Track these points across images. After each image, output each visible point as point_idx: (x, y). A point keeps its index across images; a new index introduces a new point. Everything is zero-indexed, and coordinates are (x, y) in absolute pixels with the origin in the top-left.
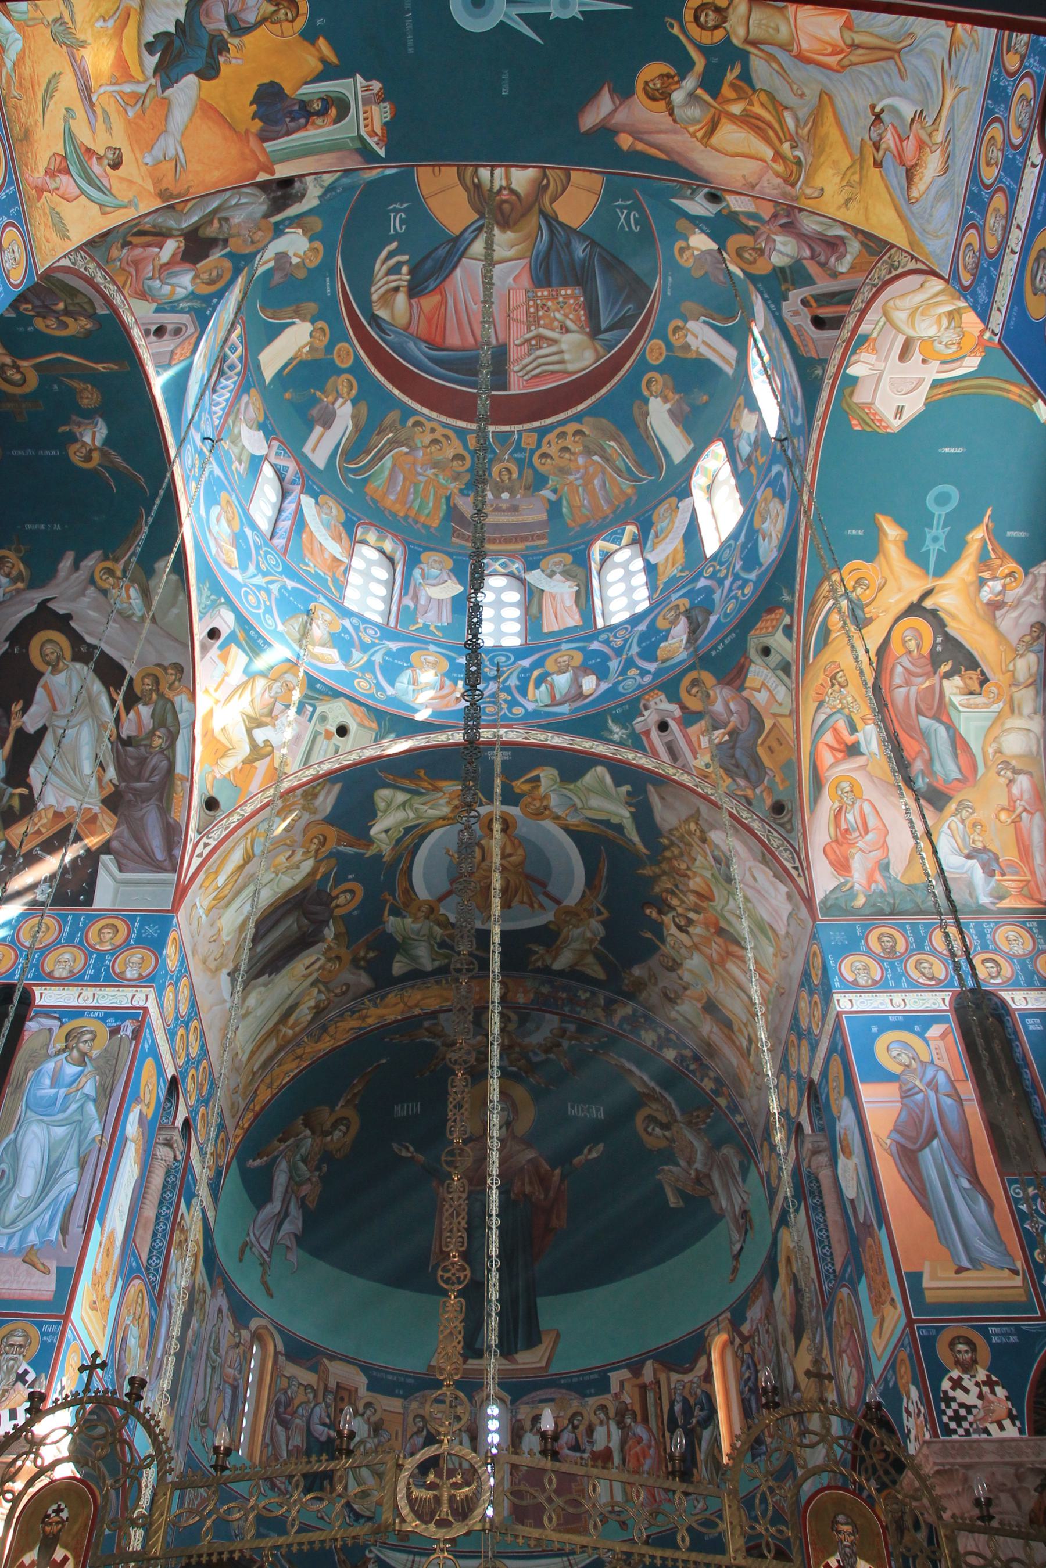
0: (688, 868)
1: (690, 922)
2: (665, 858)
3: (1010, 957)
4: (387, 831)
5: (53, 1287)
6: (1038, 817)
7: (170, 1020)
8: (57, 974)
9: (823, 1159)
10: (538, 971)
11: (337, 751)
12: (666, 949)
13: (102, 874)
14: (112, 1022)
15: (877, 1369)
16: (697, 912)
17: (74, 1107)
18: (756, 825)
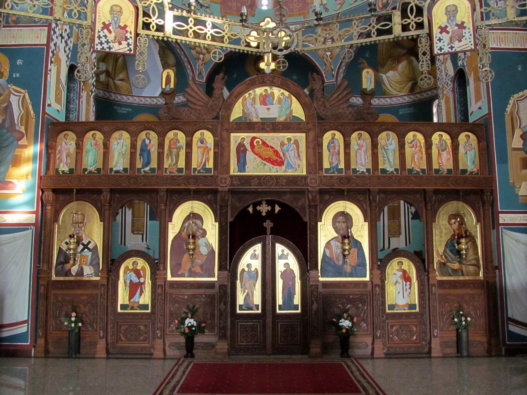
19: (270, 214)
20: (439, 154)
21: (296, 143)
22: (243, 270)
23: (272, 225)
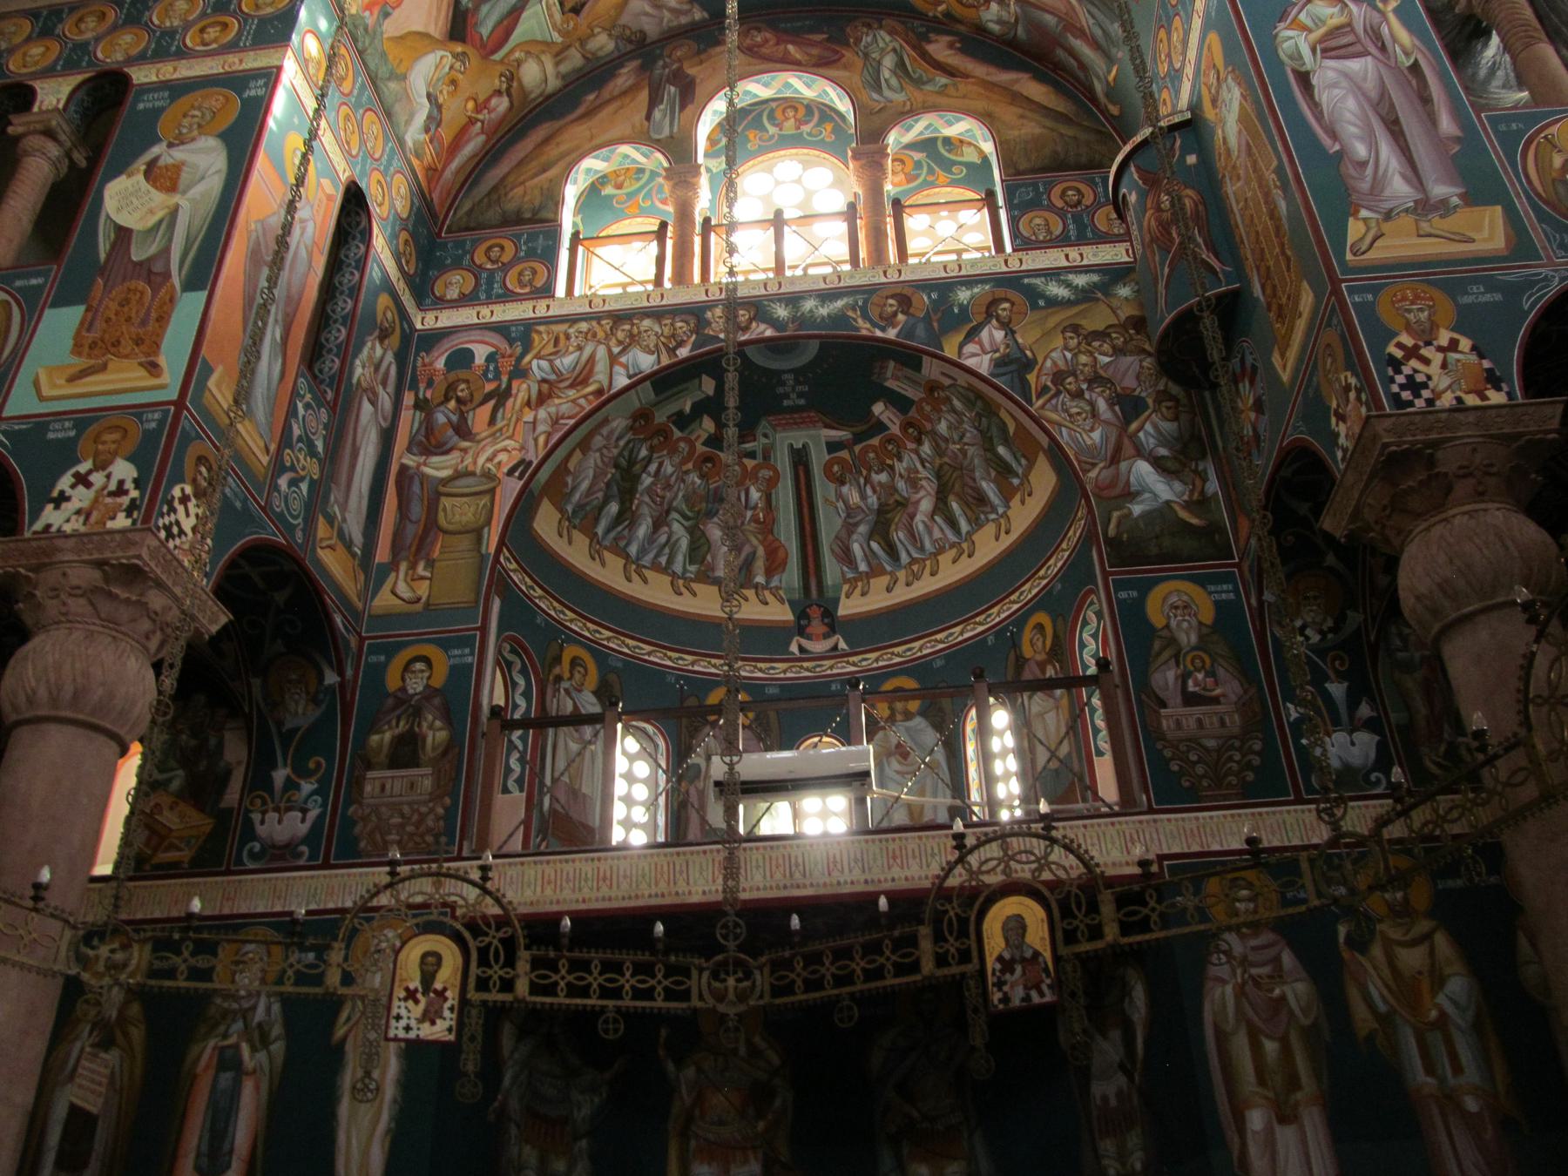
6: (482, 138)
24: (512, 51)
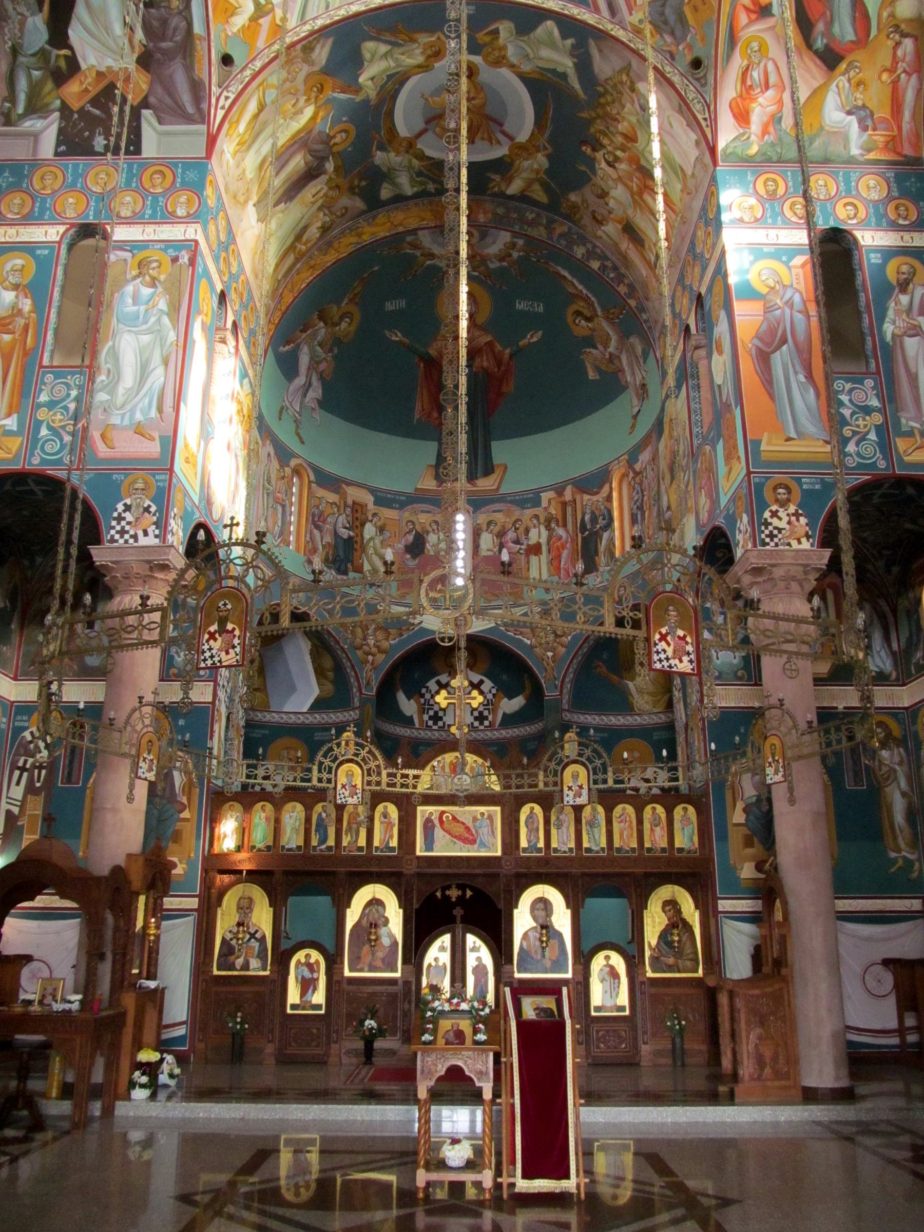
0: (618, 113)
1: (617, 159)
2: (599, 104)
3: (865, 201)
4: (372, 79)
5: (159, 449)
6: (914, 78)
7: (215, 247)
8: (123, 214)
9: (702, 353)
10: (495, 195)
11: (327, 7)
12: (597, 180)
13: (144, 126)
14: (172, 253)
15: (724, 501)
16: (623, 151)
17: (153, 319)
18: (676, 79)
19: (461, 899)
20: (652, 830)
21: (490, 818)
22: (430, 966)
23: (462, 912)
24: (879, 16)
